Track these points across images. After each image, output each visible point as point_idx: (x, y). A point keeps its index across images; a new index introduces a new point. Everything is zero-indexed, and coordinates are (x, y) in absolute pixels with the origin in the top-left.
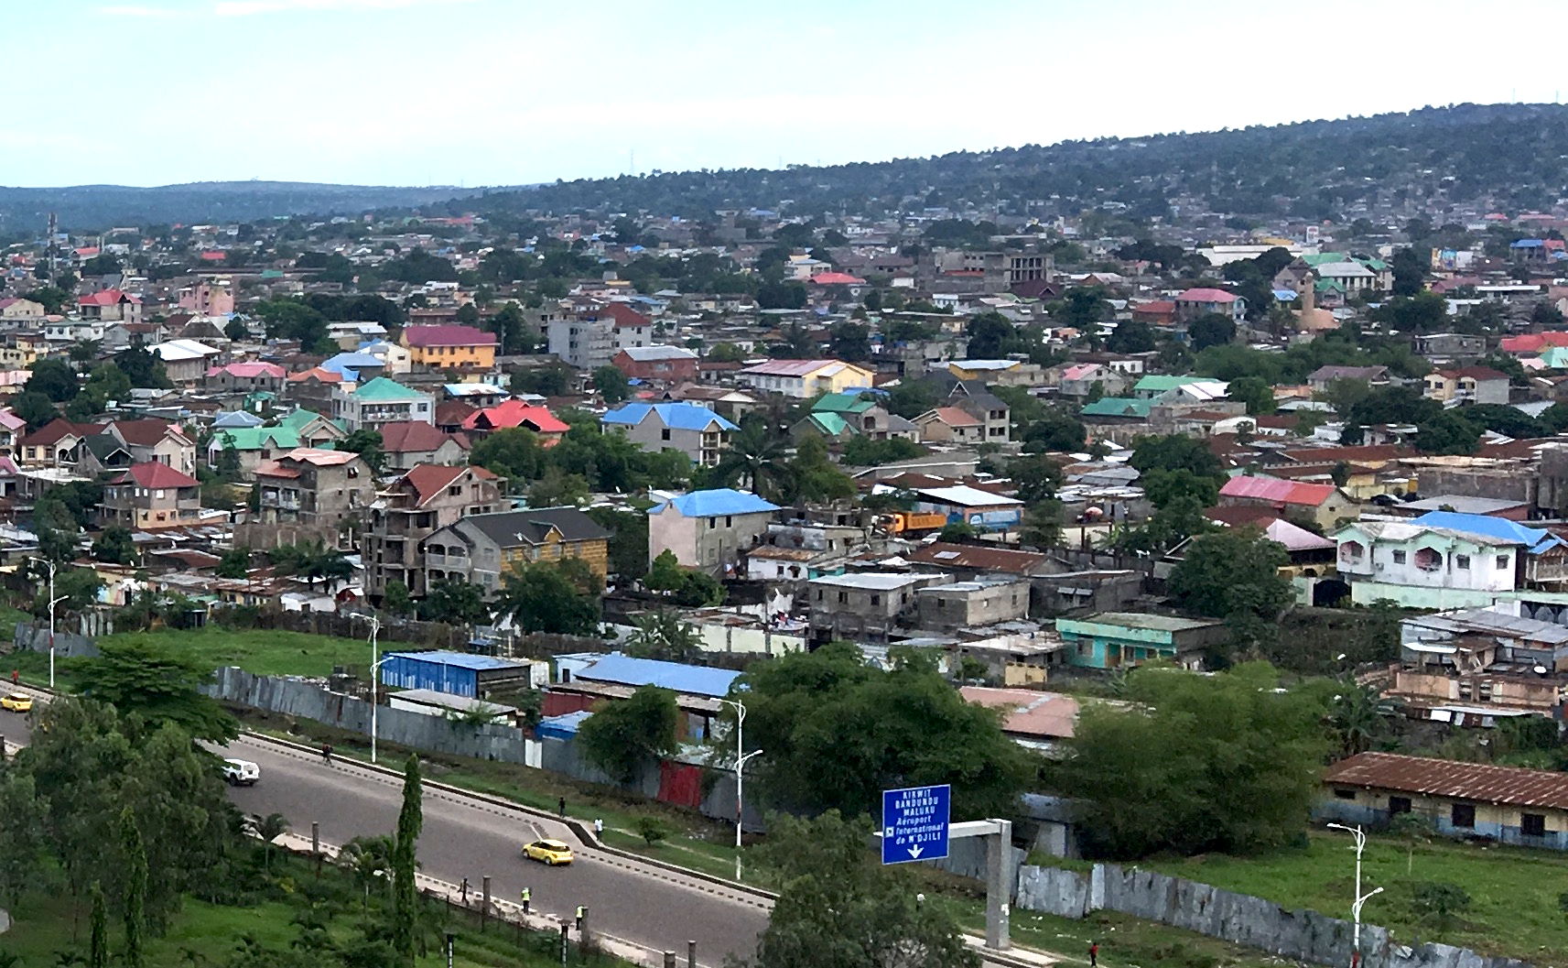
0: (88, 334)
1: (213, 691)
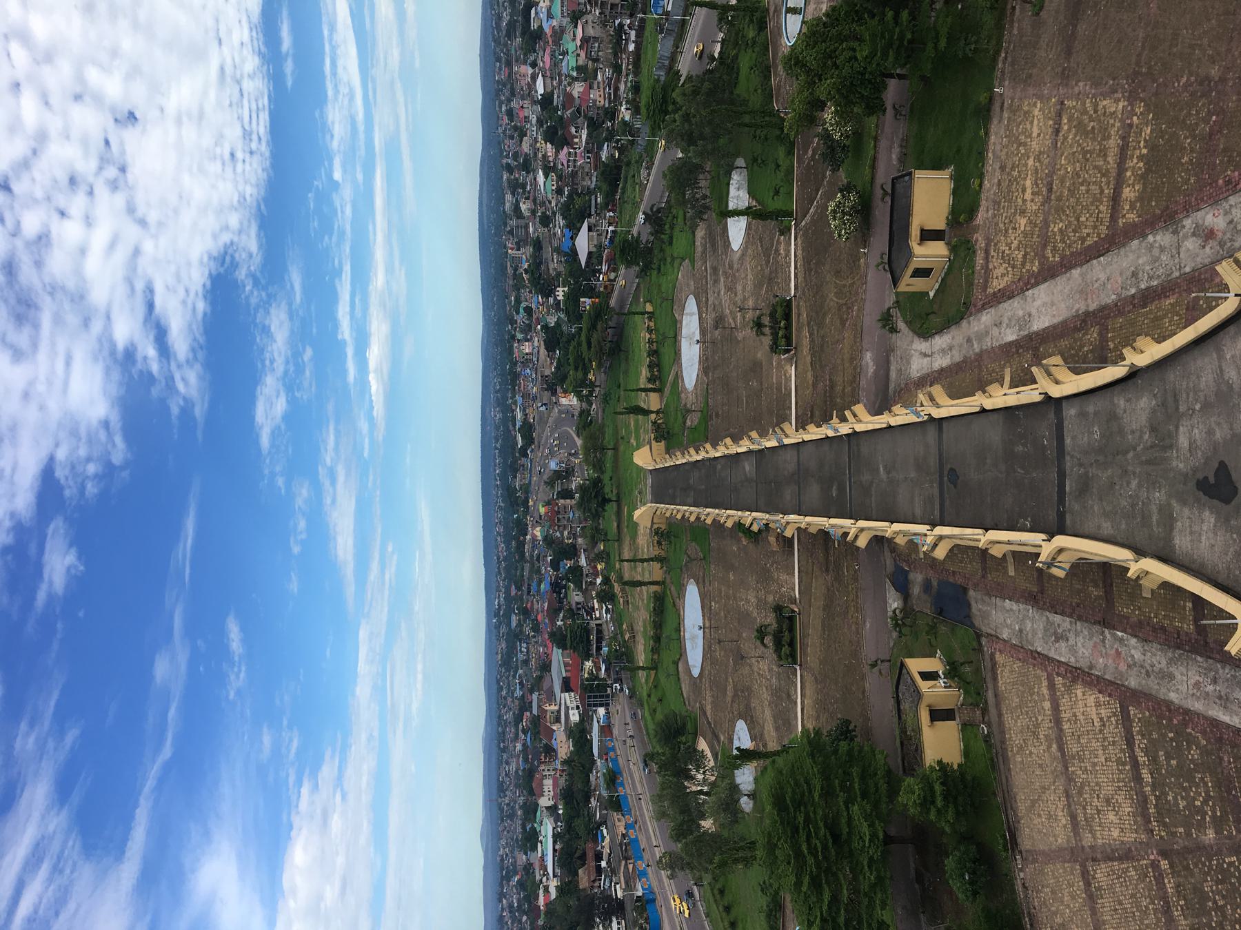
0: (534, 121)
1: (663, 78)
